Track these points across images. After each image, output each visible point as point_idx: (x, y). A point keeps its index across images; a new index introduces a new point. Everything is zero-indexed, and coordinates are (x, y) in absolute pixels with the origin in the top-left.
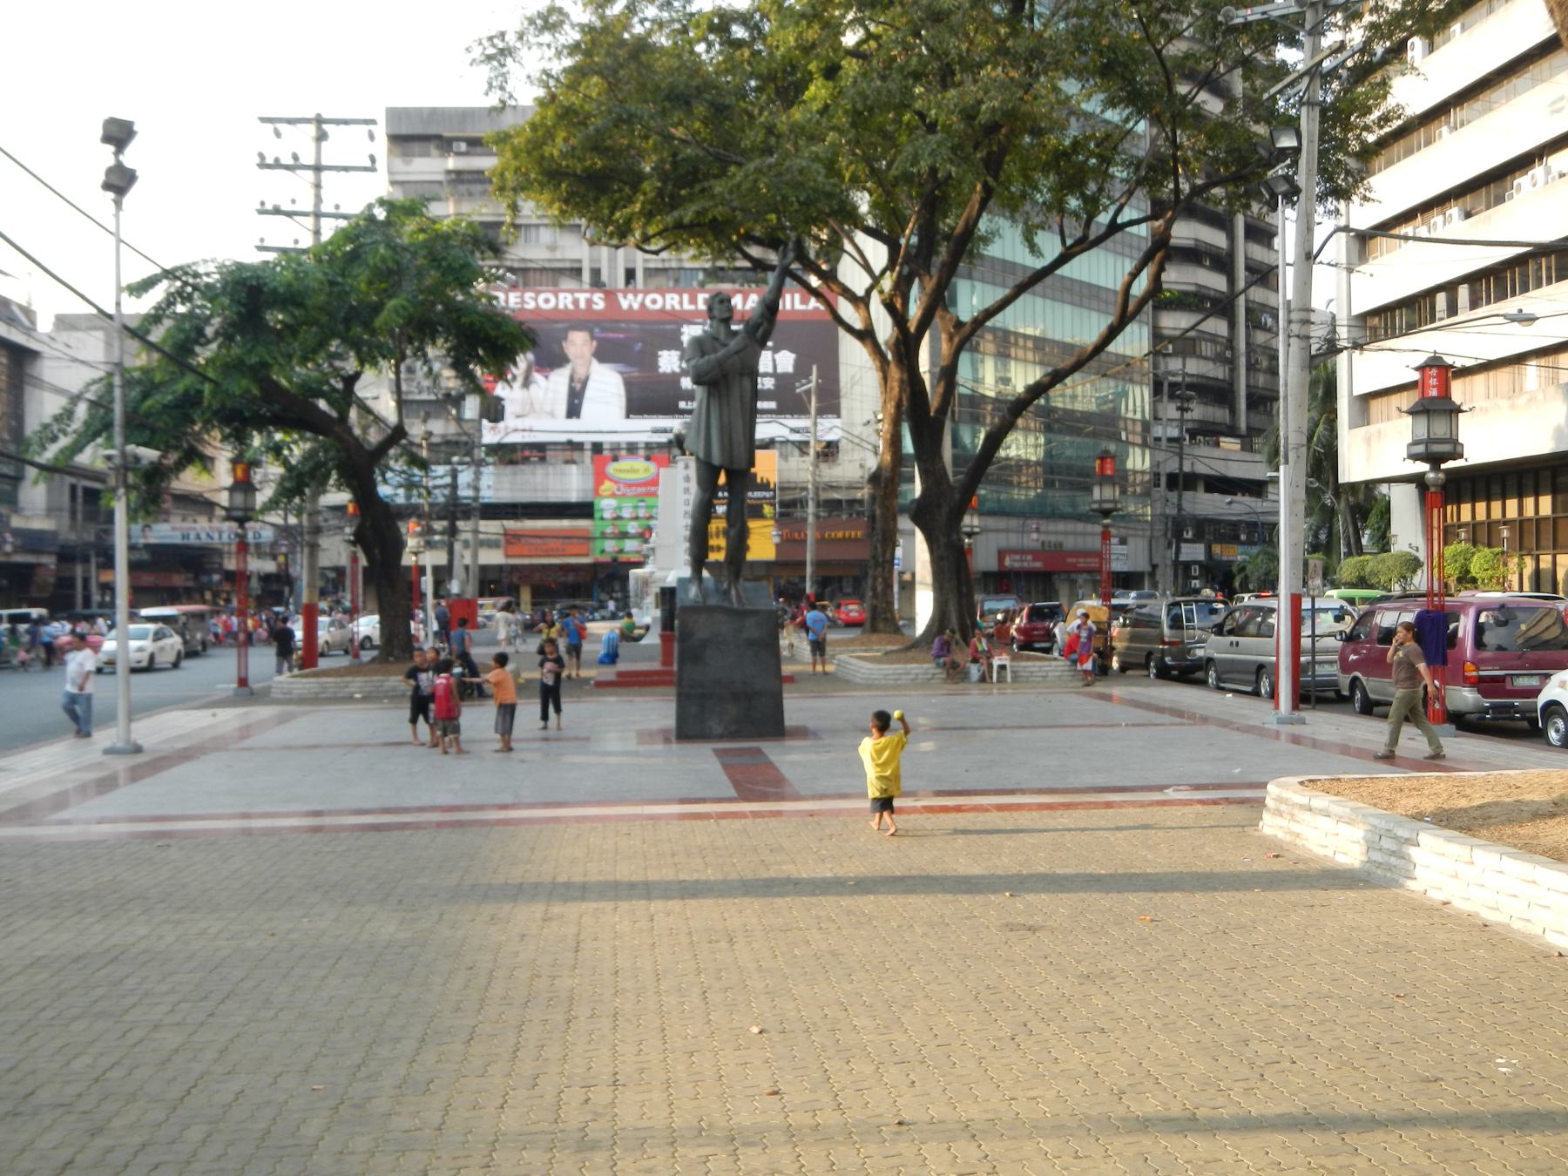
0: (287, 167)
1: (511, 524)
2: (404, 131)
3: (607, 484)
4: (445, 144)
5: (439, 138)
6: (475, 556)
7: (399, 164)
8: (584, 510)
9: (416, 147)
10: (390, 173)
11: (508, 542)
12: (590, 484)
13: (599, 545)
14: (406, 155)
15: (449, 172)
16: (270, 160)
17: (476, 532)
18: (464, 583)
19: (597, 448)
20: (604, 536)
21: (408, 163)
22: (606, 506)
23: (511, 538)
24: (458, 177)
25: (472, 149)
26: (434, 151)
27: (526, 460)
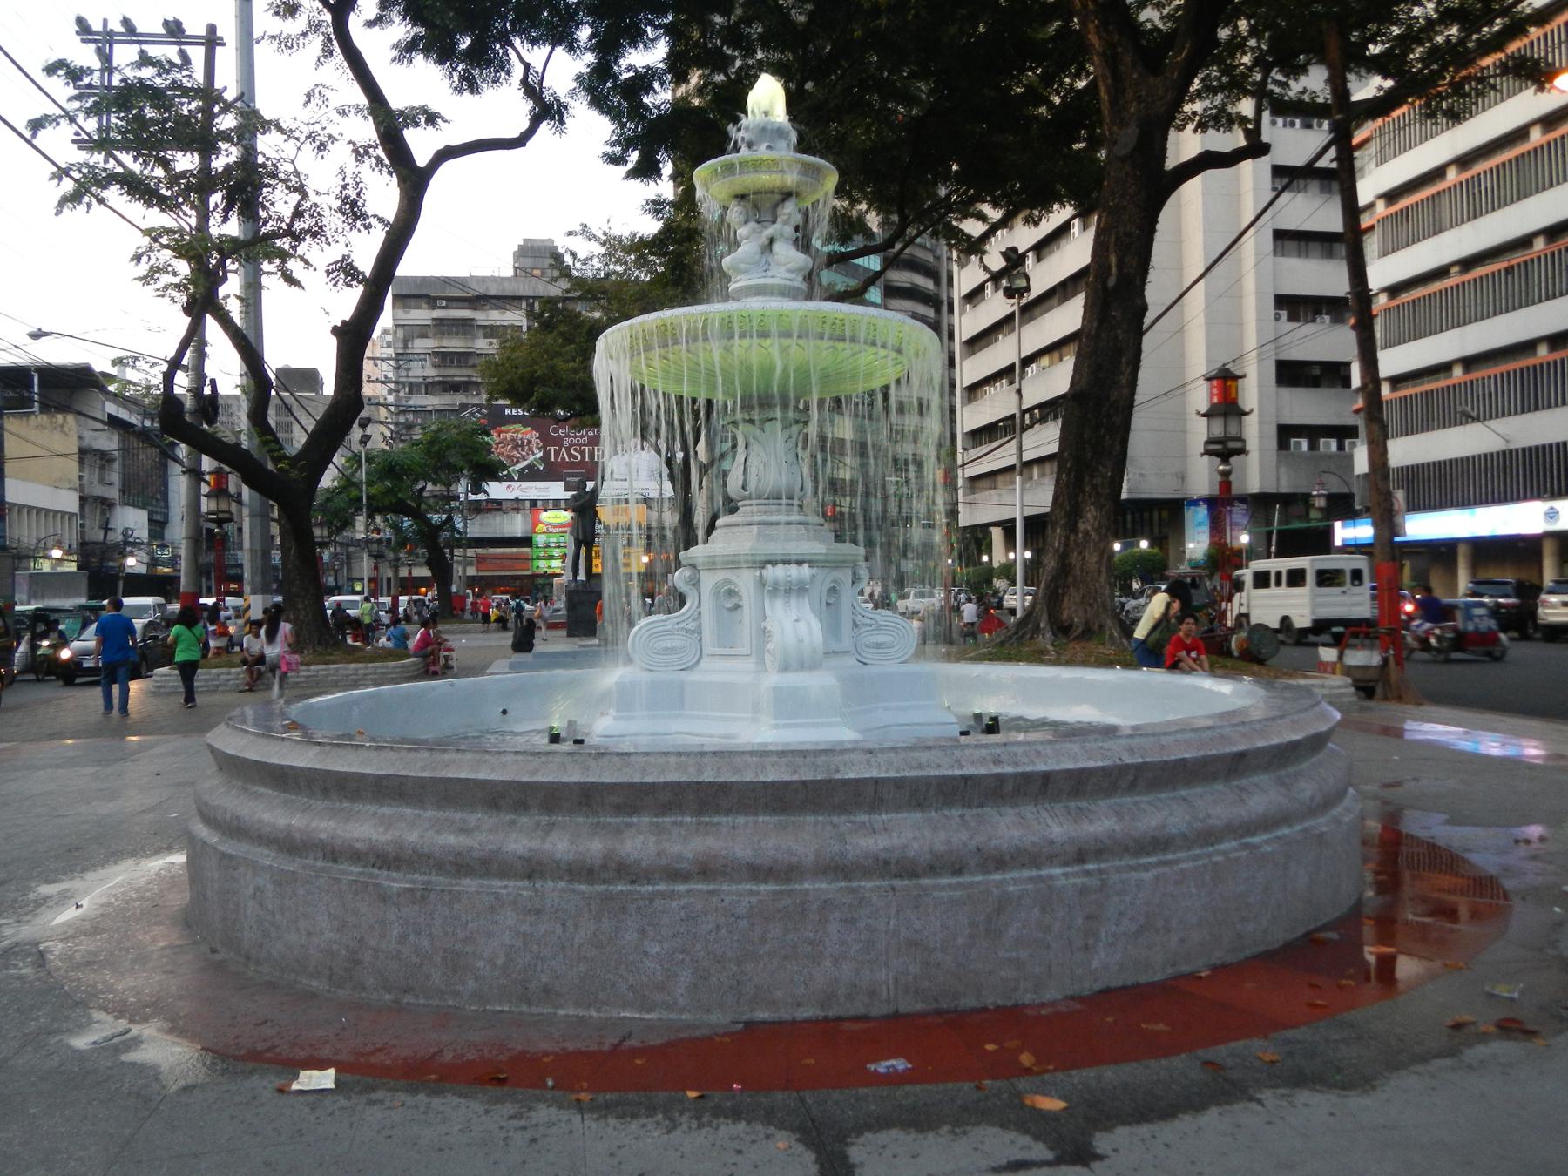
0: (382, 382)
1: (480, 551)
2: (404, 292)
3: (540, 528)
4: (432, 302)
5: (428, 296)
6: (465, 571)
7: (401, 313)
8: (526, 541)
9: (412, 302)
10: (394, 319)
11: (478, 562)
12: (529, 527)
13: (536, 563)
14: (406, 307)
15: (434, 319)
16: (373, 378)
17: (465, 557)
18: (458, 587)
19: (534, 503)
20: (539, 558)
21: (407, 313)
22: (540, 539)
23: (481, 559)
24: (439, 322)
25: (450, 304)
26: (424, 306)
27: (489, 510)
